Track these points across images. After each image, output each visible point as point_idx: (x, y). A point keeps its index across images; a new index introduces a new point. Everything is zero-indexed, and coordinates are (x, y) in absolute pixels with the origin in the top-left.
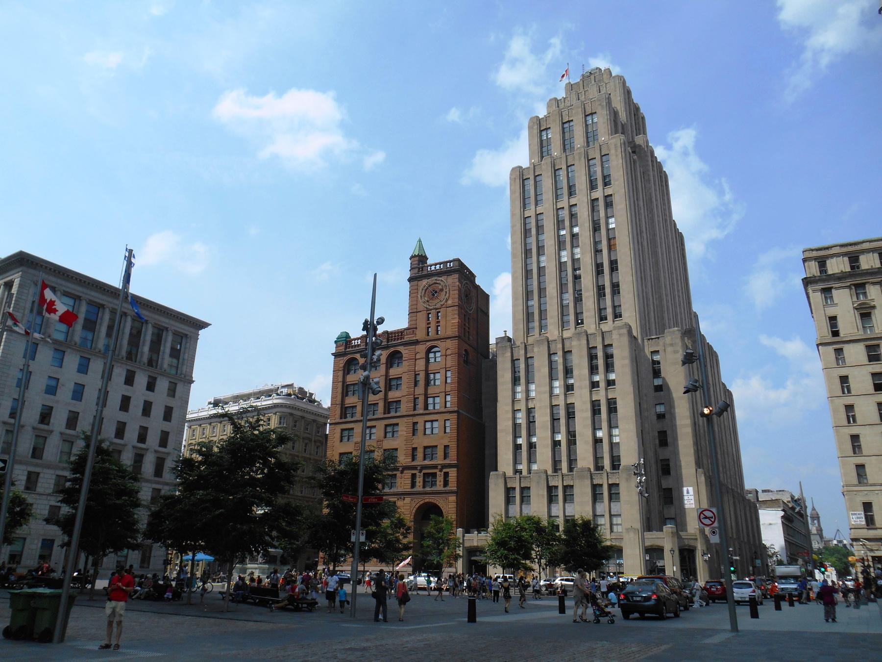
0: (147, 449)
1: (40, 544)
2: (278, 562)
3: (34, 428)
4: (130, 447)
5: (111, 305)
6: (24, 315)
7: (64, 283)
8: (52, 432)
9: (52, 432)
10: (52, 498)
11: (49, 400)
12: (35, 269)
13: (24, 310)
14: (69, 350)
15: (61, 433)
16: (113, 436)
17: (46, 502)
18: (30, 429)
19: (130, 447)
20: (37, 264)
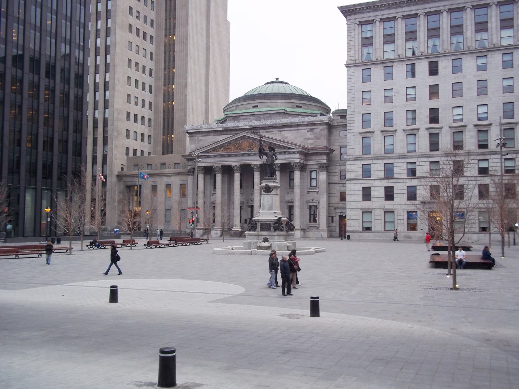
0: (490, 125)
1: (406, 216)
2: (272, 229)
3: (382, 132)
4: (470, 127)
5: (423, 11)
6: (355, 51)
7: (378, 13)
8: (396, 131)
9: (396, 131)
10: (407, 180)
11: (388, 107)
12: (355, 14)
13: (355, 48)
14: (395, 64)
15: (404, 130)
16: (452, 121)
17: (404, 184)
18: (379, 132)
19: (470, 127)
20: (353, 10)
